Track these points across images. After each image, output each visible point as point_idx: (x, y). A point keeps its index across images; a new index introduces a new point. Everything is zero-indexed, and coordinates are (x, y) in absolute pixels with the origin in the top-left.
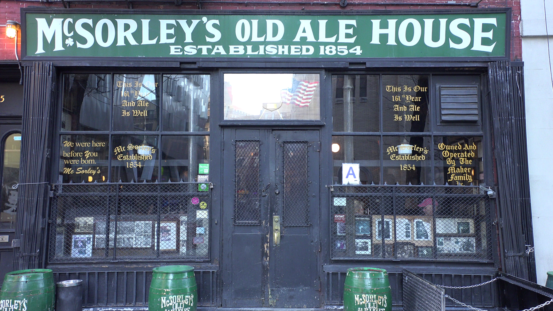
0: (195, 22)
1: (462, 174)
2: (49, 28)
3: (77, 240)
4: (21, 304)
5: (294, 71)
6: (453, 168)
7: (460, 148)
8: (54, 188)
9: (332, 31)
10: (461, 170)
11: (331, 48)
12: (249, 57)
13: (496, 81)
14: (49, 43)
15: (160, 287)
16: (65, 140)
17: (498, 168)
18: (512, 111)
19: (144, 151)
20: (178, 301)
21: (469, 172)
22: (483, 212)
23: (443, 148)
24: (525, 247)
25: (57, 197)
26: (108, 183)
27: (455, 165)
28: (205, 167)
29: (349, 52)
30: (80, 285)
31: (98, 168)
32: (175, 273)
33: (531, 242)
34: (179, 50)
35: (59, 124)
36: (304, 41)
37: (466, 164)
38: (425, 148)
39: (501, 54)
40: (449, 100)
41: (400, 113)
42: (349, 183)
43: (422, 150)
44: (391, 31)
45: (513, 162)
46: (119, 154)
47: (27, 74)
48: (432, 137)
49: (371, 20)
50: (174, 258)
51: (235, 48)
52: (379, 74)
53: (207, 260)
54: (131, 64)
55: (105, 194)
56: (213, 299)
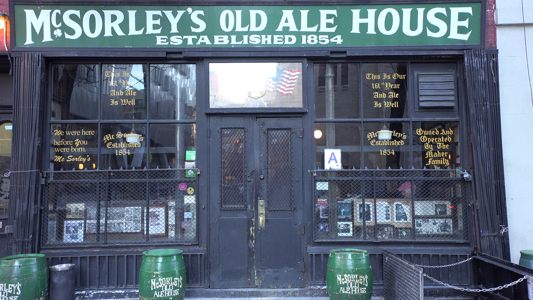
0: (180, 13)
1: (439, 158)
2: (38, 19)
3: (69, 225)
4: (15, 288)
5: (277, 60)
6: (431, 153)
7: (437, 133)
8: (45, 176)
9: (314, 20)
10: (439, 154)
11: (312, 37)
12: (233, 46)
13: (471, 68)
14: (38, 34)
15: (150, 270)
16: (56, 129)
17: (474, 152)
18: (487, 96)
19: (133, 139)
20: (167, 284)
21: (446, 156)
22: (459, 195)
23: (421, 133)
24: (500, 227)
25: (49, 184)
26: (98, 170)
27: (432, 149)
28: (192, 154)
29: (330, 41)
30: (72, 268)
31: (88, 156)
32: (164, 257)
33: (505, 223)
34: (165, 40)
35: (49, 114)
36: (286, 31)
37: (443, 148)
38: (404, 133)
39: (477, 42)
40: (426, 87)
41: (380, 100)
42: (331, 168)
43: (401, 135)
44: (370, 20)
45: (488, 146)
46: (108, 142)
48: (411, 123)
49: (351, 10)
50: (163, 242)
51: (219, 38)
52: (359, 63)
53: (195, 243)
54: (119, 54)
55: (95, 181)
56: (201, 281)
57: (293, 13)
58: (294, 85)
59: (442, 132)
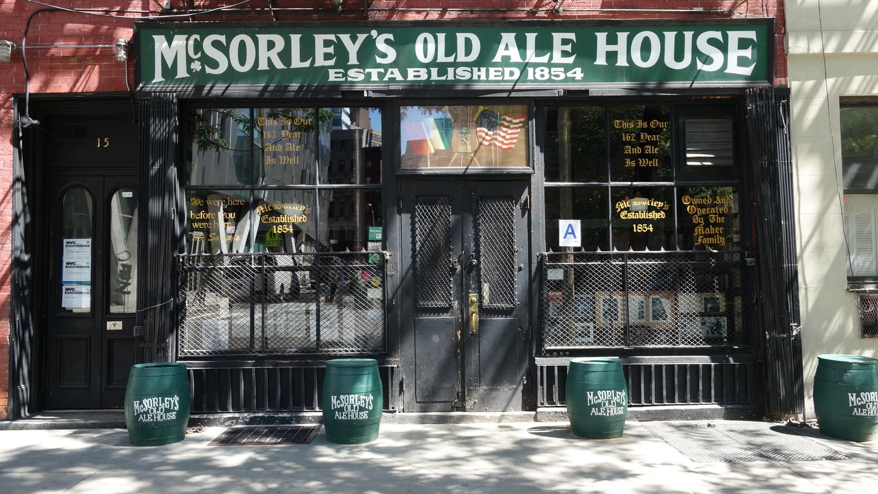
0: (362, 37)
1: (710, 236)
2: (170, 47)
10: (712, 230)
11: (542, 71)
12: (433, 83)
20: (351, 403)
22: (738, 284)
28: (377, 231)
29: (566, 76)
34: (341, 75)
41: (632, 157)
47: (143, 110)
51: (414, 71)
57: (516, 37)
58: (517, 136)
59: (715, 200)
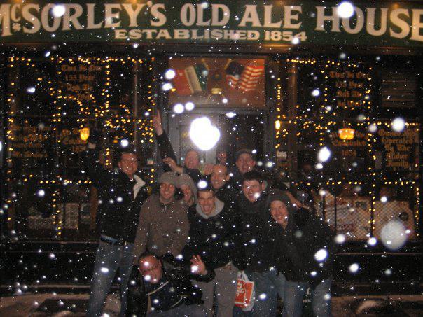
0: (140, 6)
9: (278, 16)
10: (398, 156)
11: (276, 33)
34: (124, 34)
36: (249, 26)
57: (257, 9)
